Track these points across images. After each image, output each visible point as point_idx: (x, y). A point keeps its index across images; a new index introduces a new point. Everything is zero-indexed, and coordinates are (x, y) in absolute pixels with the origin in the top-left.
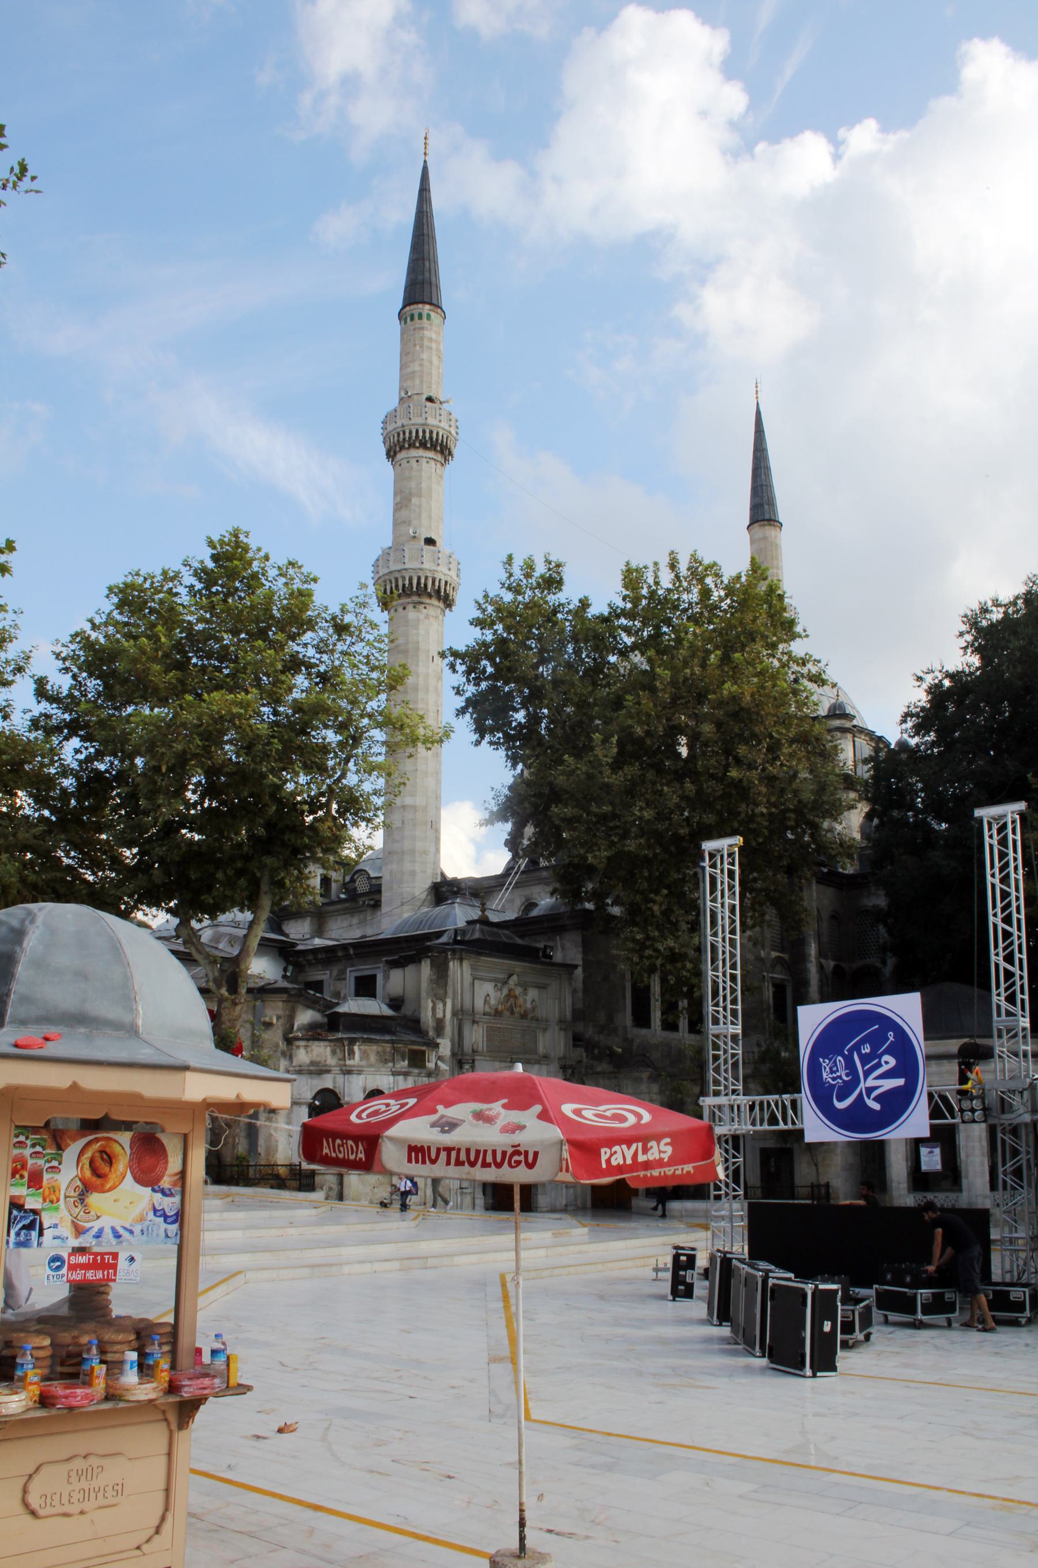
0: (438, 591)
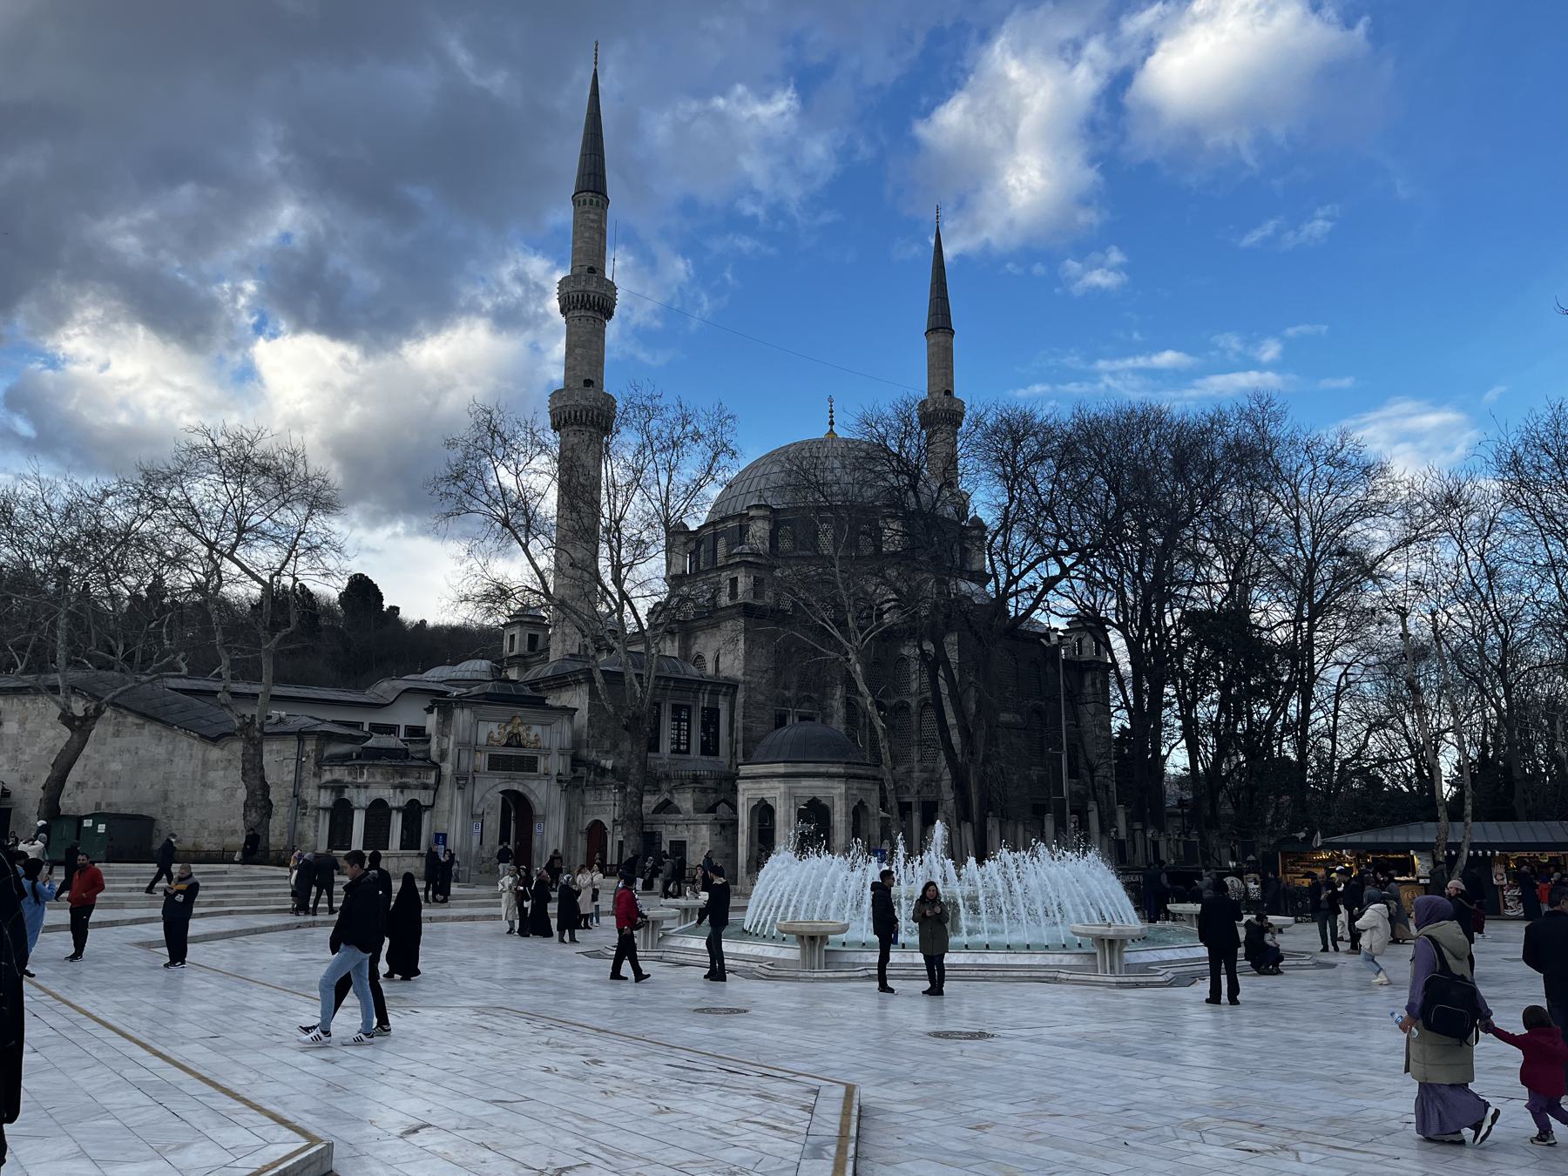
0: (592, 421)
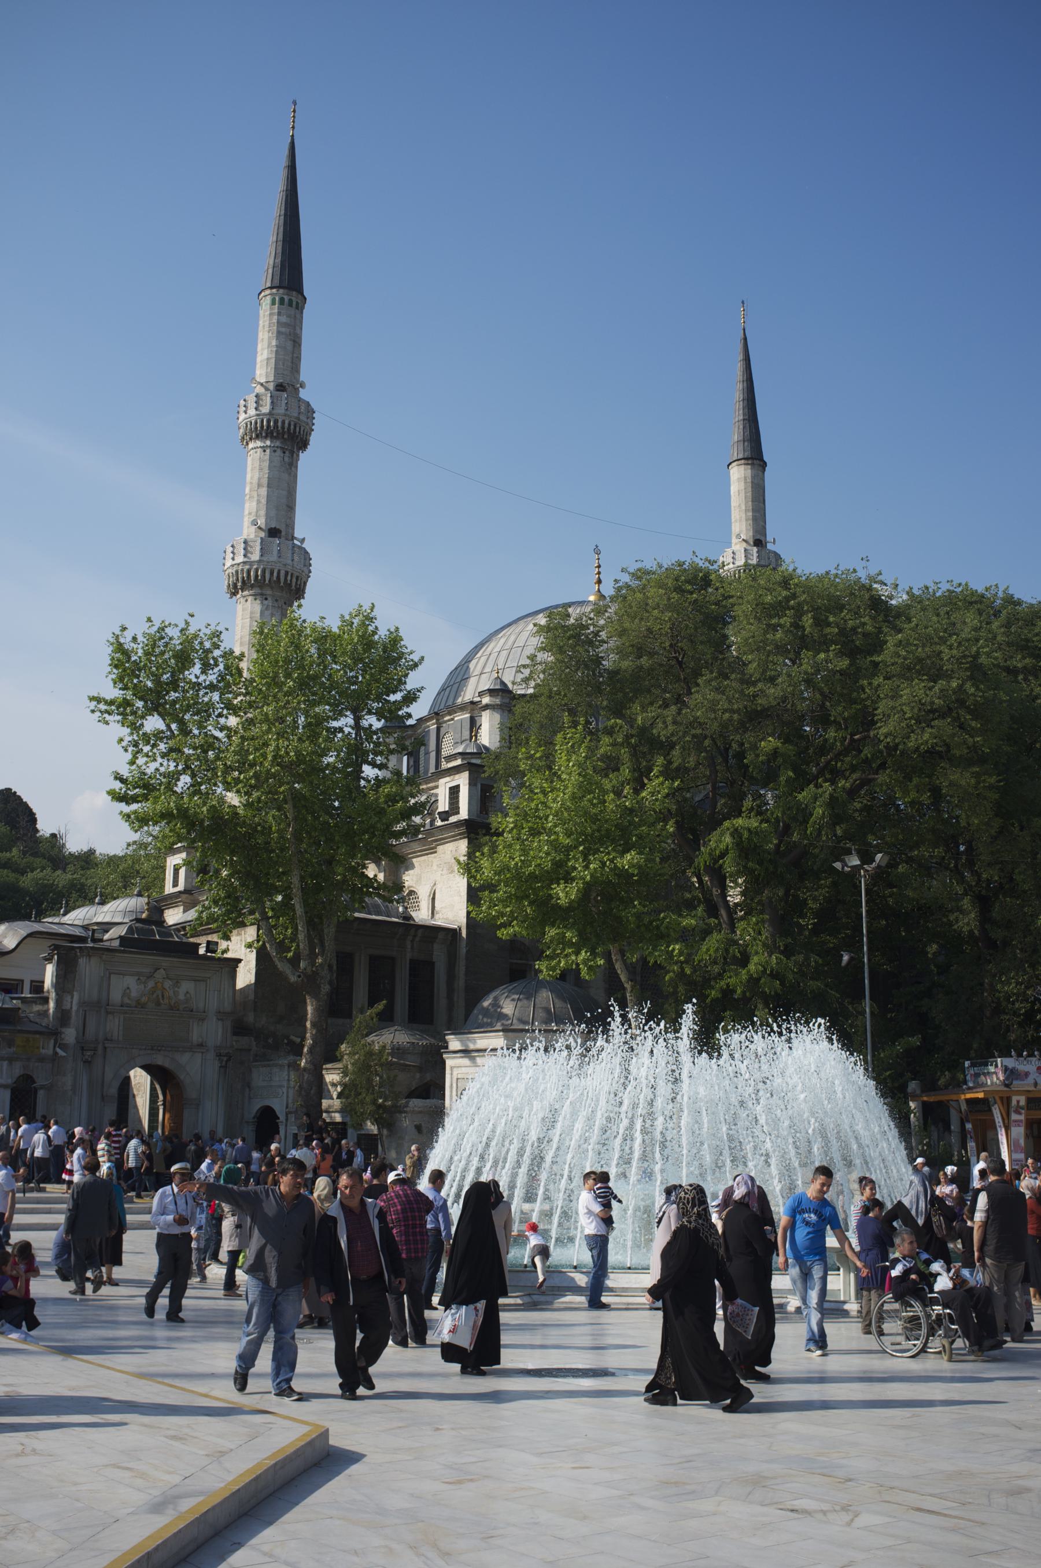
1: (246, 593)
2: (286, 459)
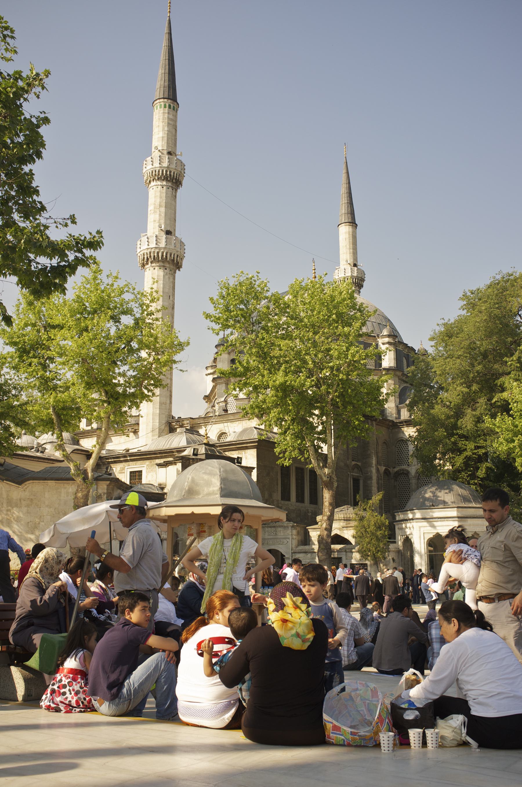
0: (173, 260)
1: (154, 265)
2: (174, 193)
